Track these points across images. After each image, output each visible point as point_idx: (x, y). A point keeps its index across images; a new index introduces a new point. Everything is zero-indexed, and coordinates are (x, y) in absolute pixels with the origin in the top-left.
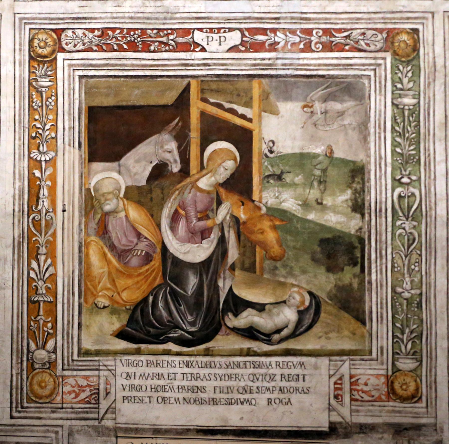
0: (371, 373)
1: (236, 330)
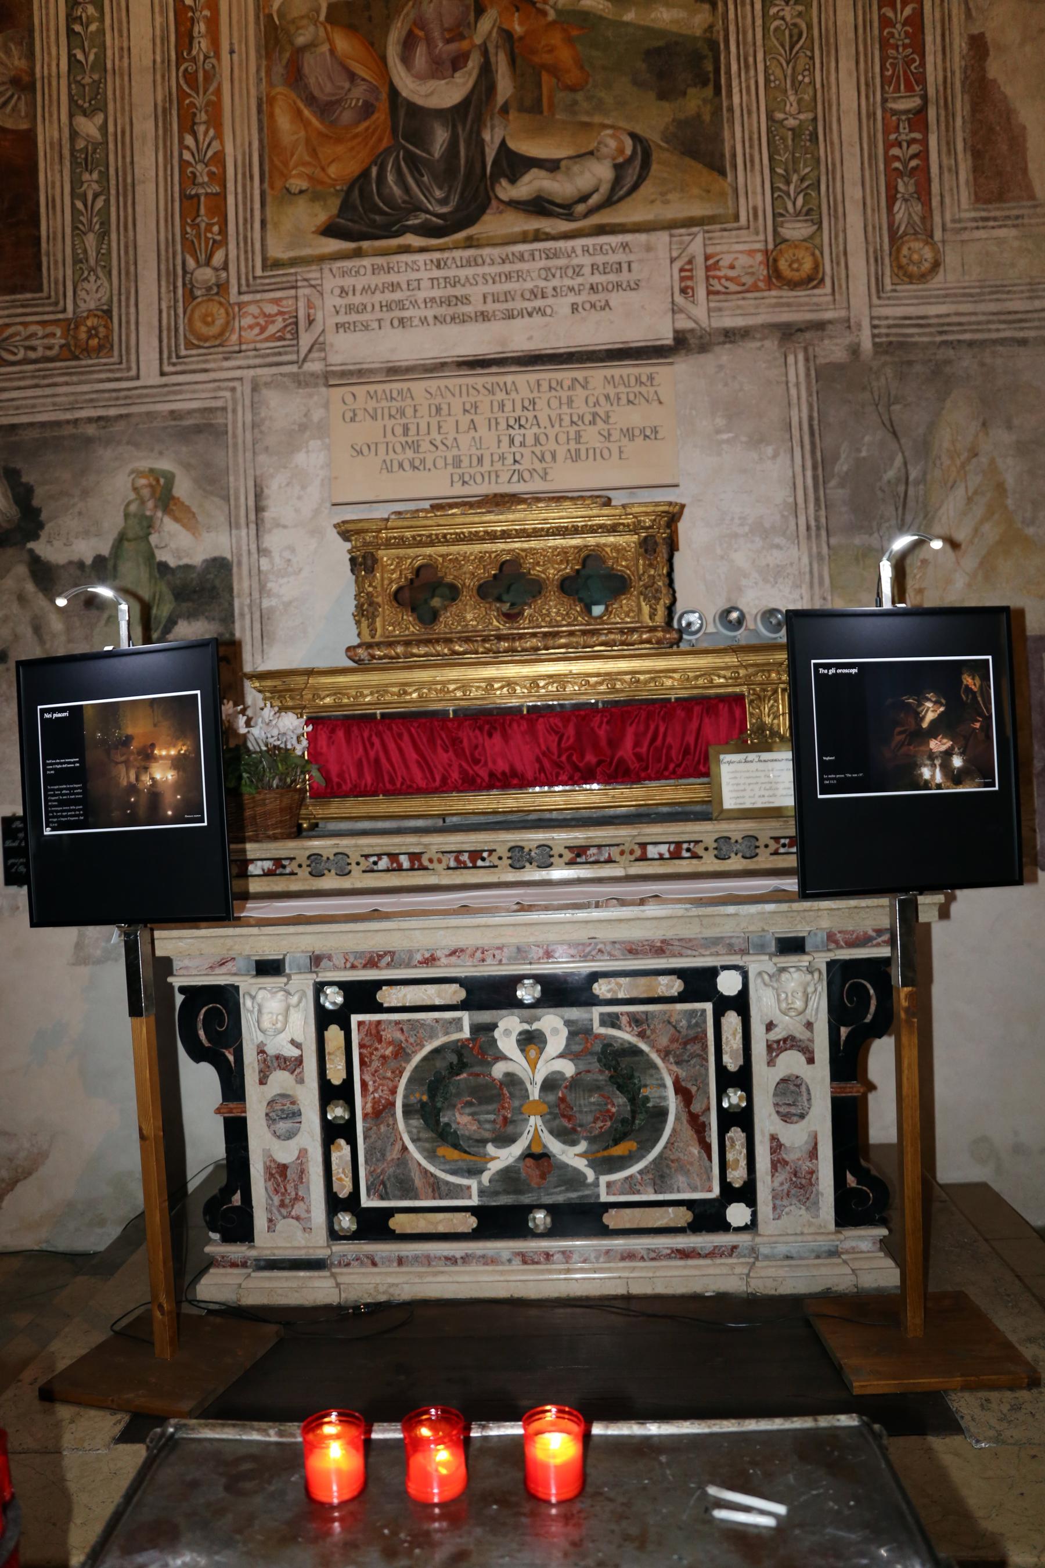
1: (515, 205)
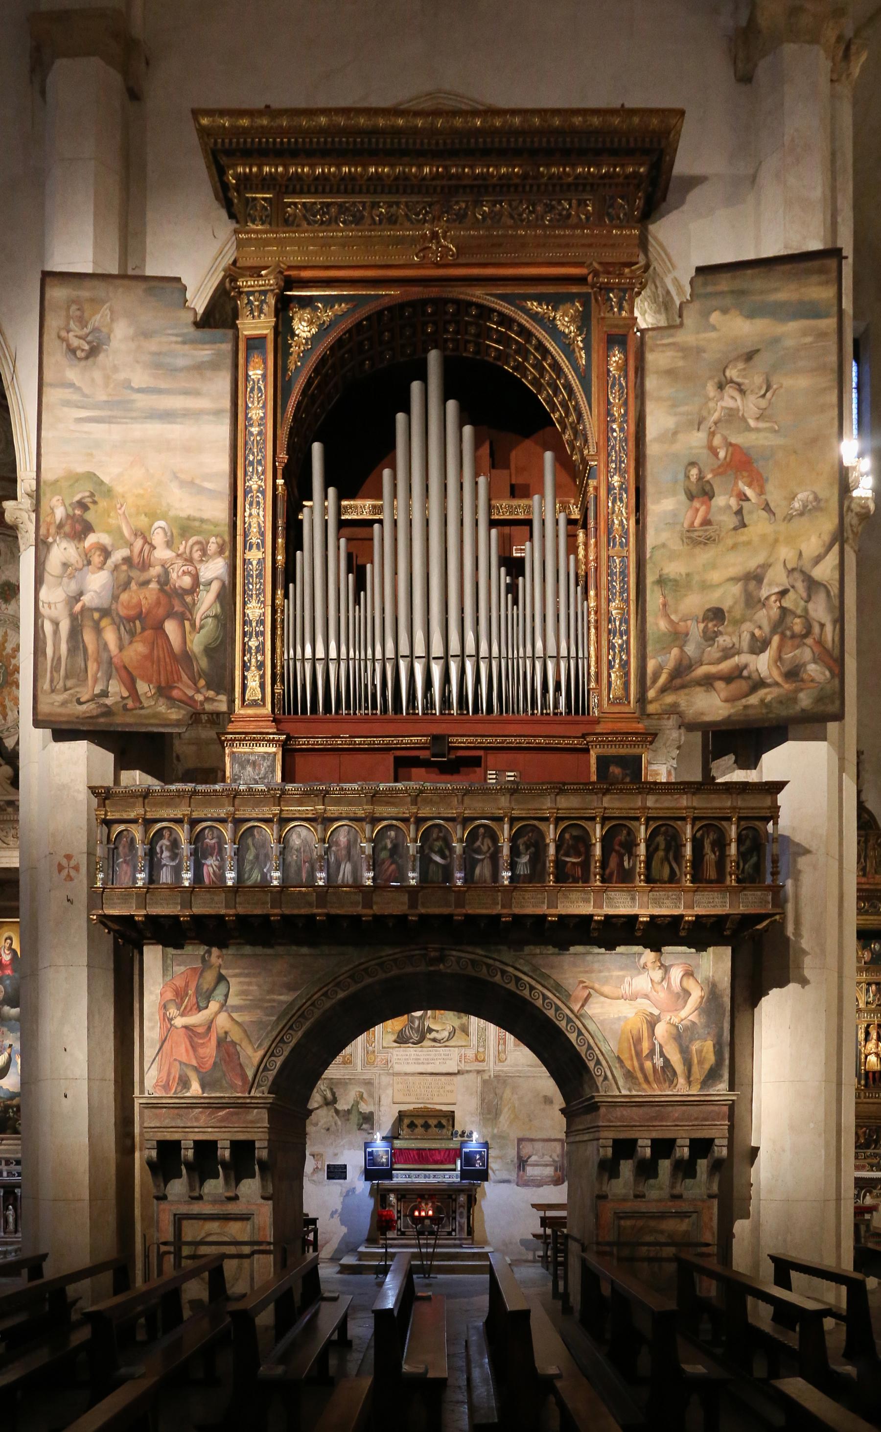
0: (471, 1053)
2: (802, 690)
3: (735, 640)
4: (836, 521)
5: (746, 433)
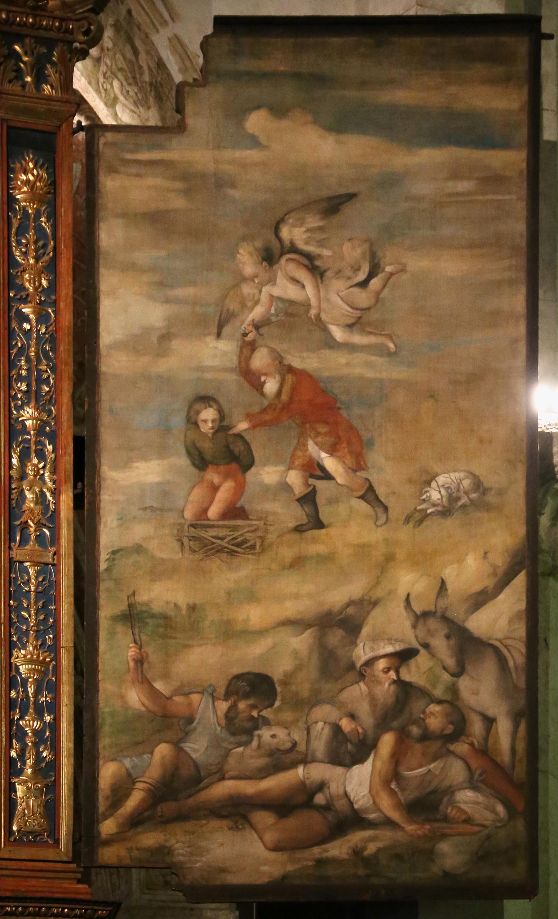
2: (444, 836)
3: (298, 735)
4: (522, 531)
5: (327, 353)
